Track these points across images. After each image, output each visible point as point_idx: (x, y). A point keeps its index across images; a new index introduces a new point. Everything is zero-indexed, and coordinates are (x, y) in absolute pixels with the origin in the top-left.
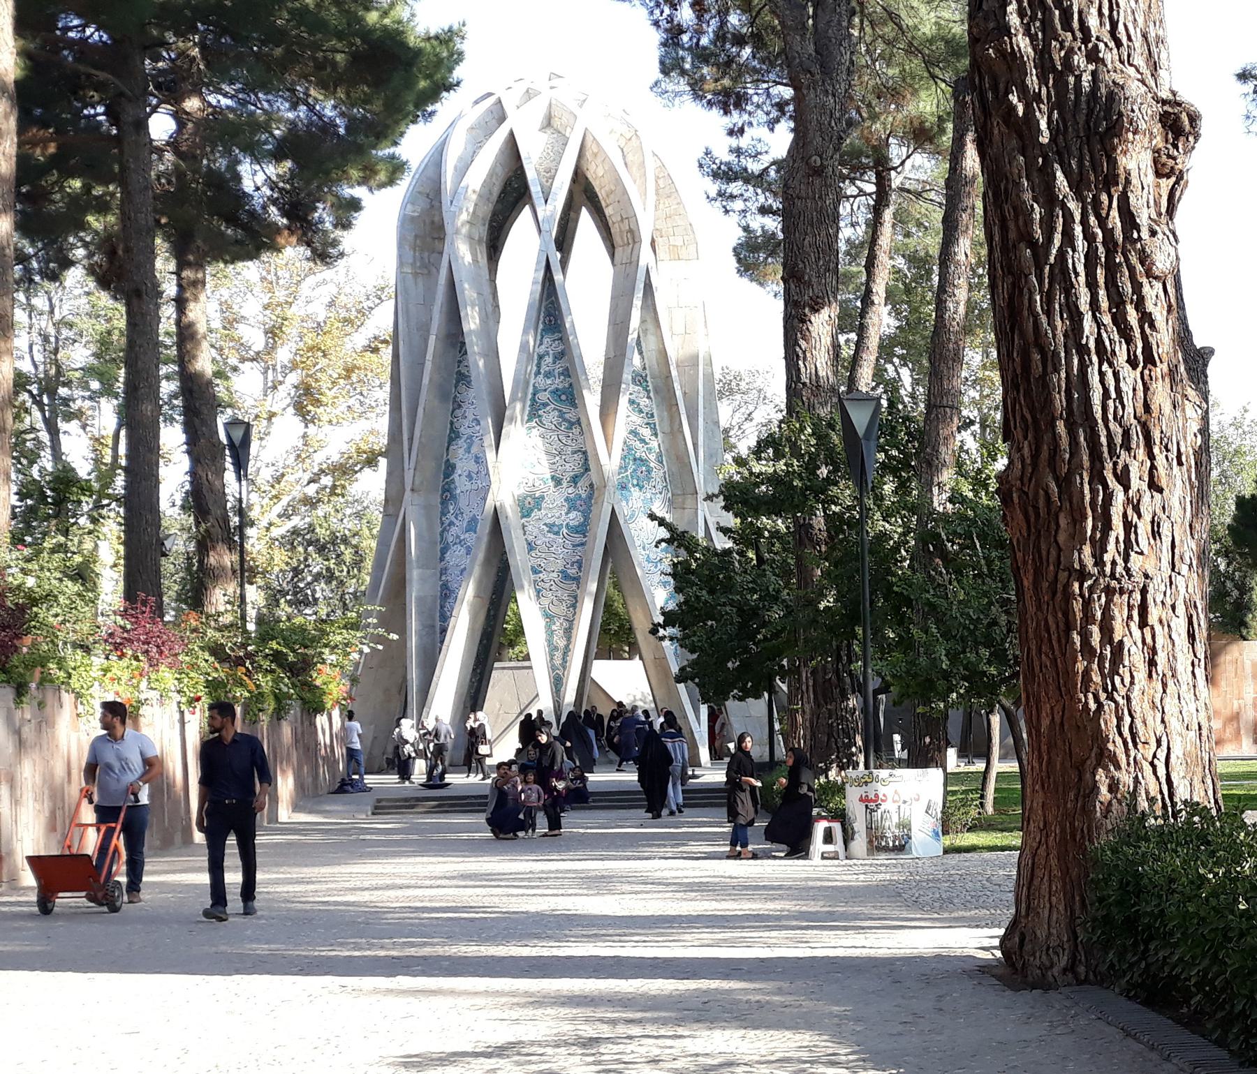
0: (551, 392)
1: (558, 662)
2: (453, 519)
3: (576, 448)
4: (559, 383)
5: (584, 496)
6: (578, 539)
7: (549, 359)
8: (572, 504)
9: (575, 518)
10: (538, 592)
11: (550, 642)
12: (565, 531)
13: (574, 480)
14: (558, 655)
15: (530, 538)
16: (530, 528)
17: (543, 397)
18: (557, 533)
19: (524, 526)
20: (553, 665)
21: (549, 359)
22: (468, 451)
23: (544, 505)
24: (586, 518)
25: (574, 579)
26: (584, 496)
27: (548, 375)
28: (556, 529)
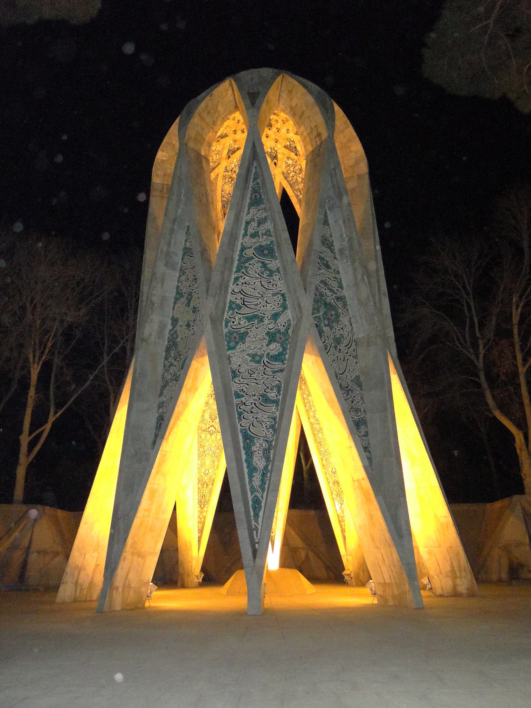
0: (255, 249)
1: (257, 482)
2: (173, 361)
3: (275, 291)
4: (264, 241)
5: (283, 330)
6: (278, 365)
7: (254, 224)
8: (272, 337)
9: (275, 348)
10: (240, 414)
11: (249, 461)
12: (266, 359)
13: (275, 316)
14: (257, 477)
15: (235, 367)
16: (233, 359)
17: (249, 252)
18: (259, 362)
19: (229, 358)
20: (252, 487)
21: (254, 224)
22: (189, 302)
23: (247, 339)
24: (284, 349)
25: (273, 402)
26: (283, 330)
27: (255, 235)
28: (257, 358)
